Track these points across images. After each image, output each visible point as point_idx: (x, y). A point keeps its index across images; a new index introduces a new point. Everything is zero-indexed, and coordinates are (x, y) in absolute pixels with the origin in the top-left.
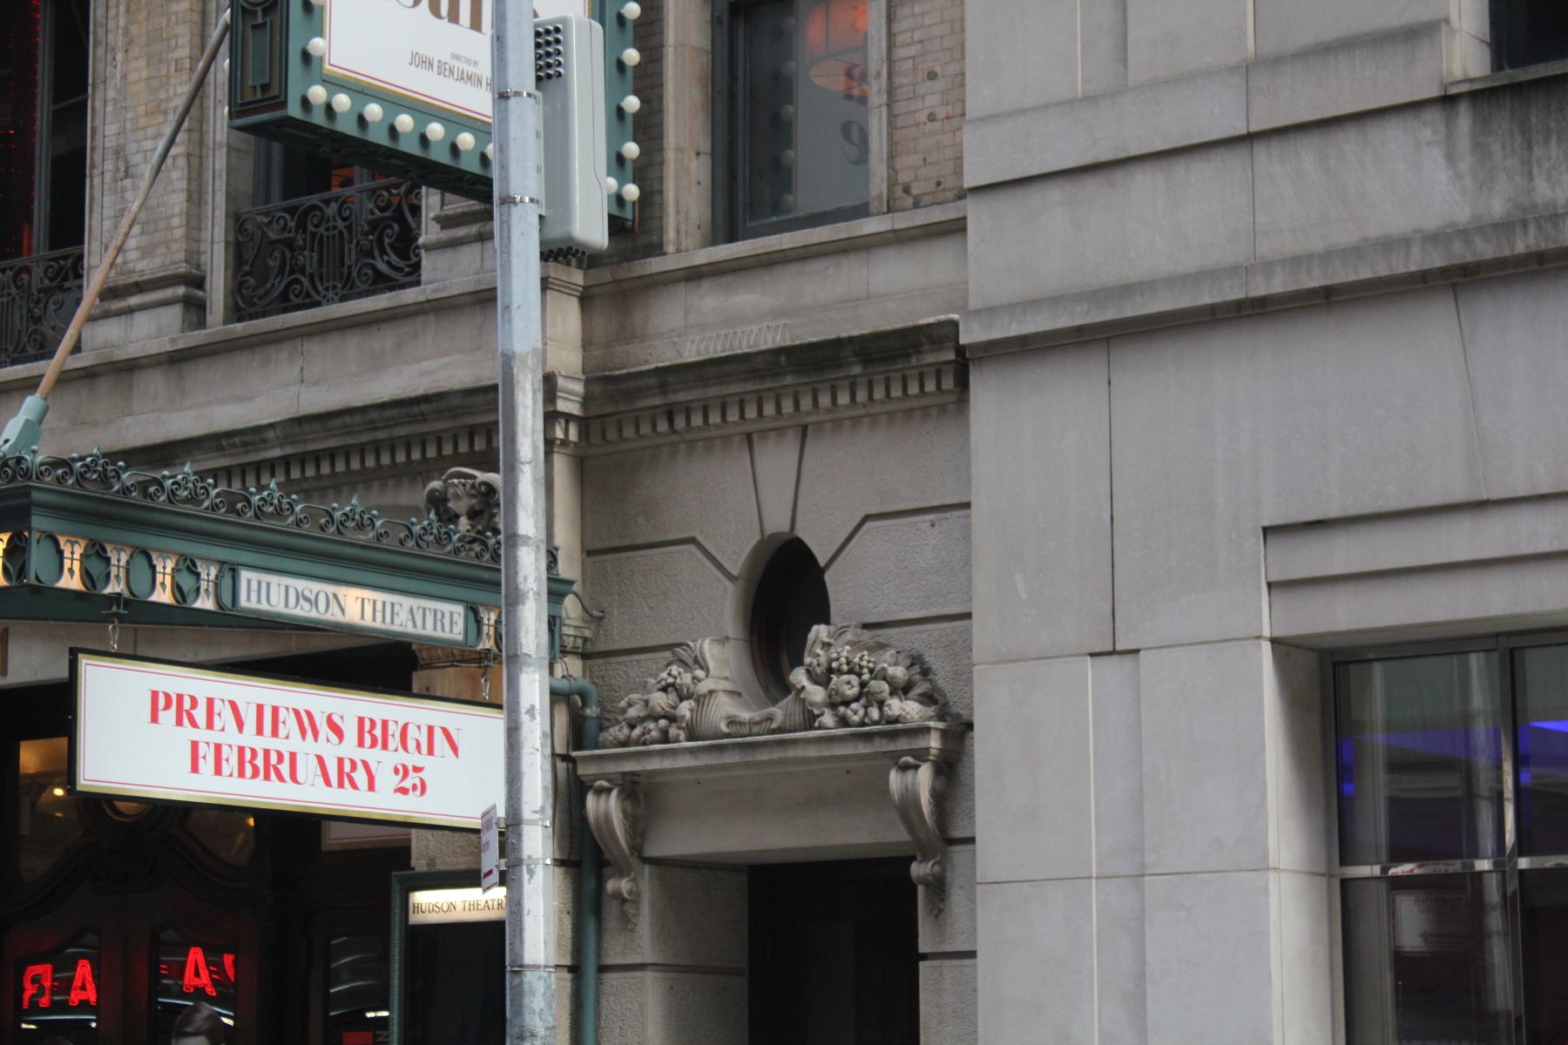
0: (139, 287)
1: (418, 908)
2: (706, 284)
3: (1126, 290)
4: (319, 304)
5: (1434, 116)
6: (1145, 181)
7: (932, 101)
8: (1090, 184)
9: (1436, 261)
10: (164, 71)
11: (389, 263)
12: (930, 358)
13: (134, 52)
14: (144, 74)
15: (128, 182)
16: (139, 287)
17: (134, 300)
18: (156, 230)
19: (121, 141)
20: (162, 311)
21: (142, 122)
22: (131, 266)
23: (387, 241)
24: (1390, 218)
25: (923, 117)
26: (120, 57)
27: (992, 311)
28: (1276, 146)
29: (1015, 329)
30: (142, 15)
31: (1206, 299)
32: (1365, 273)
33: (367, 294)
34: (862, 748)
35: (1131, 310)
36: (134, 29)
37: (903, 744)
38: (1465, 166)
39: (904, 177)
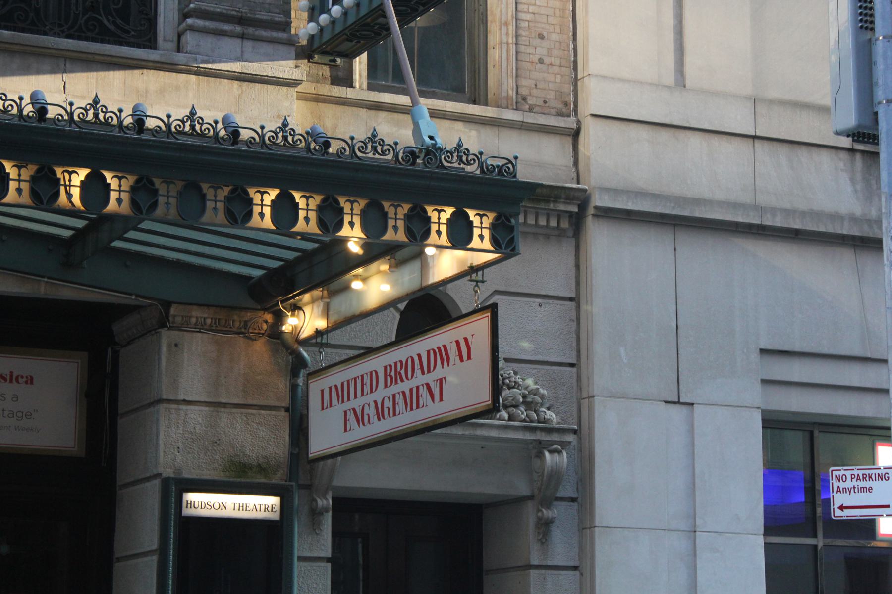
1: (191, 505)
2: (383, 115)
3: (697, 202)
4: (45, 34)
5: (844, 155)
6: (695, 140)
7: (541, 51)
8: (664, 135)
9: (856, 232)
11: (114, 23)
12: (562, 207)
23: (112, 7)
24: (824, 202)
25: (535, 59)
27: (616, 192)
28: (766, 144)
29: (630, 206)
31: (740, 219)
32: (822, 229)
34: (529, 436)
35: (699, 213)
37: (555, 437)
38: (859, 187)
39: (524, 91)
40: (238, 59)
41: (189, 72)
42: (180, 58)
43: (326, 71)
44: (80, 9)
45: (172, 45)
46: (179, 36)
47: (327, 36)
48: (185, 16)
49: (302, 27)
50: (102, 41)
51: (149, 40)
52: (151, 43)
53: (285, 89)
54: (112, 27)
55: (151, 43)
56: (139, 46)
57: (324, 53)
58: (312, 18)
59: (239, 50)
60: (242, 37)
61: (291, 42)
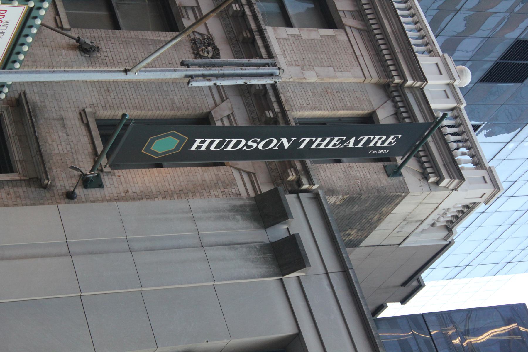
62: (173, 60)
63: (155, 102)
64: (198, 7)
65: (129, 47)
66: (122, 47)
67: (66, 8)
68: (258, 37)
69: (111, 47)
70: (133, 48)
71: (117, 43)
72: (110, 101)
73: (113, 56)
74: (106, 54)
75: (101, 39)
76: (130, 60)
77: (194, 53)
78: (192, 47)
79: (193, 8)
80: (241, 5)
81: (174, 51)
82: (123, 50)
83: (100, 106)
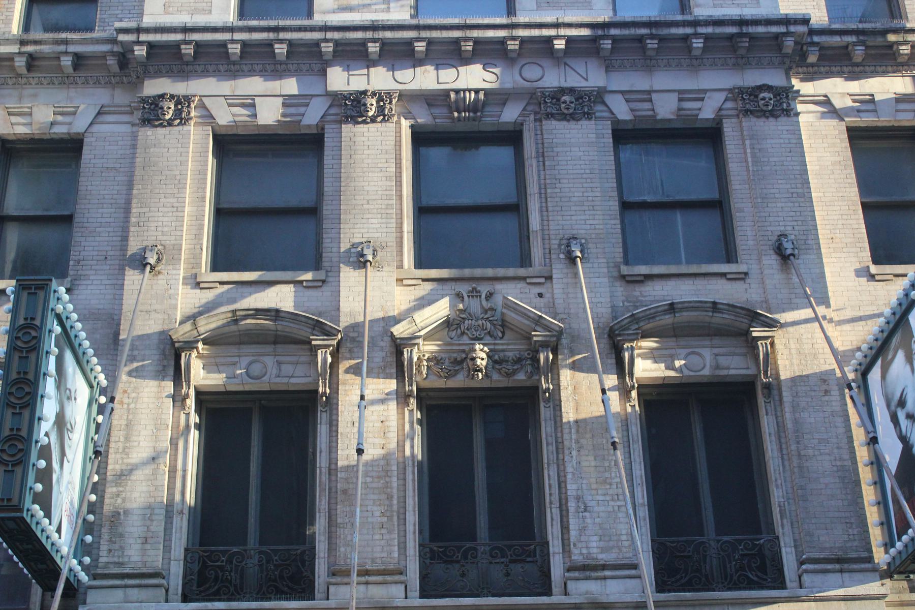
0: (604, 567)
10: (607, 464)
11: (757, 576)
13: (583, 452)
14: (593, 463)
15: (587, 514)
16: (604, 567)
17: (607, 573)
18: (610, 540)
19: (580, 493)
20: (628, 580)
21: (594, 486)
22: (595, 556)
23: (753, 565)
26: (574, 453)
30: (589, 436)
33: (745, 589)
36: (583, 441)
40: (841, 587)
41: (810, 601)
42: (802, 592)
43: (905, 584)
44: (733, 570)
45: (796, 584)
46: (800, 577)
47: (898, 562)
48: (802, 563)
49: (881, 557)
50: (751, 589)
51: (780, 584)
52: (782, 585)
53: (877, 601)
54: (755, 579)
55: (782, 585)
56: (774, 588)
57: (900, 573)
58: (887, 552)
59: (840, 581)
60: (841, 571)
61: (875, 570)
62: (783, 146)
63: (842, 185)
64: (680, 92)
65: (772, 196)
66: (774, 205)
67: (679, 263)
68: (751, 29)
69: (777, 219)
70: (772, 191)
71: (766, 209)
72: (850, 240)
73: (791, 219)
74: (789, 228)
75: (765, 229)
76: (794, 200)
77: (767, 117)
78: (758, 117)
79: (680, 100)
80: (696, 35)
81: (768, 141)
82: (779, 205)
83: (861, 254)
